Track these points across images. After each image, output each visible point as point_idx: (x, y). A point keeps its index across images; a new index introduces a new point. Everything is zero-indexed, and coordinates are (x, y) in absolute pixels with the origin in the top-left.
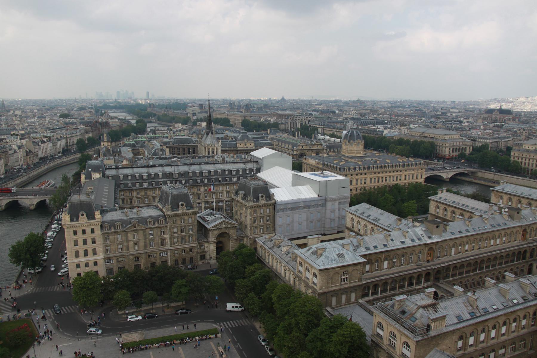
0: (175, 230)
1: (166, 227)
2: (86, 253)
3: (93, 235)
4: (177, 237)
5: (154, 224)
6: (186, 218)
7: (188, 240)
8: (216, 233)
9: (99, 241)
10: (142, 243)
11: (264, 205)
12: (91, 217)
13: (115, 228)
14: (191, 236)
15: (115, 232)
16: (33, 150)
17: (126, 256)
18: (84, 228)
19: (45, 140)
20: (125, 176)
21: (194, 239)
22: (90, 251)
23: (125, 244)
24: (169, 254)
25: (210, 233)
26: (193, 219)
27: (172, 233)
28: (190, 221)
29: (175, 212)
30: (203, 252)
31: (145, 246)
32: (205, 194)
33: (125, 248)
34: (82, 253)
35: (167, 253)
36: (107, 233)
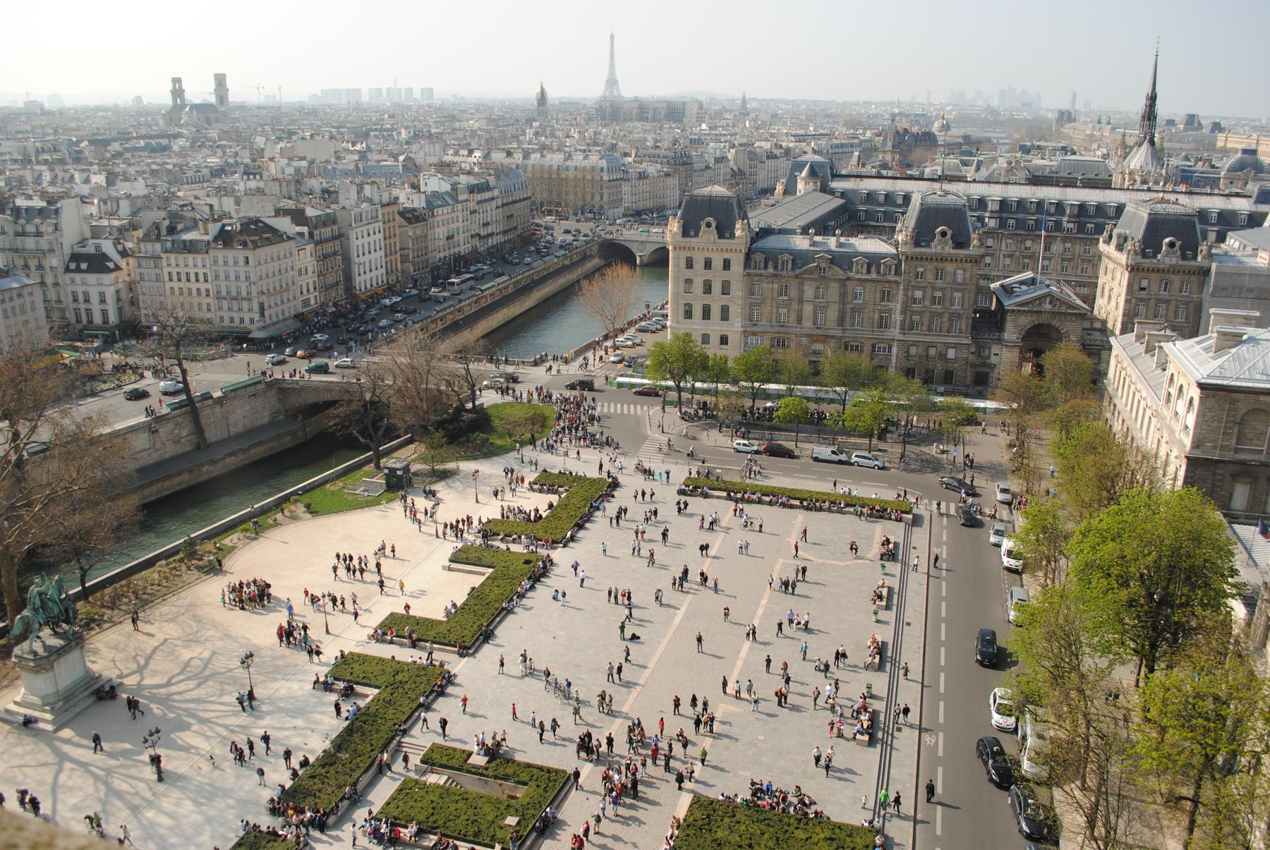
0: (918, 294)
1: (898, 283)
2: (706, 313)
3: (726, 276)
4: (920, 313)
5: (869, 272)
6: (950, 267)
7: (946, 325)
8: (1026, 321)
9: (737, 290)
10: (833, 313)
11: (1173, 270)
12: (724, 230)
13: (776, 268)
14: (955, 316)
15: (775, 276)
16: (747, 171)
17: (793, 337)
18: (708, 255)
19: (777, 152)
20: (871, 197)
21: (964, 327)
22: (716, 312)
23: (795, 307)
24: (894, 350)
25: (1009, 318)
26: (968, 275)
27: (909, 302)
28: (959, 279)
29: (923, 250)
30: (984, 364)
31: (841, 321)
32: (1063, 260)
33: (793, 317)
34: (697, 312)
35: (890, 348)
36: (757, 275)
